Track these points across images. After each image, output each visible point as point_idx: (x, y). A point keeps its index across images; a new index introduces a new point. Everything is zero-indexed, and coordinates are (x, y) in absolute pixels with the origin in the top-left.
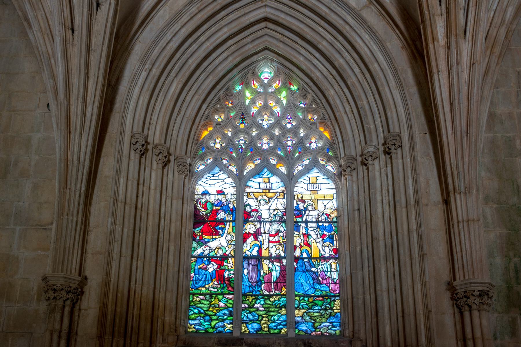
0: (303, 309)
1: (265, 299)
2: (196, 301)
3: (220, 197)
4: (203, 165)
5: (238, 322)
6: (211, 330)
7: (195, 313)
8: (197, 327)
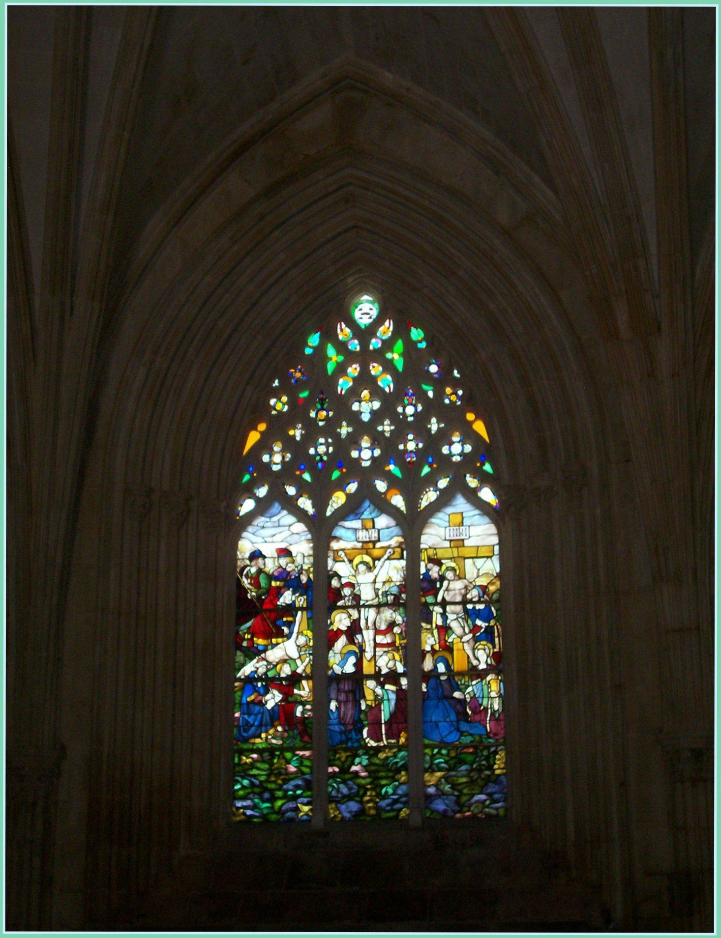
0: (440, 770)
2: (246, 763)
3: (283, 561)
4: (250, 498)
6: (273, 817)
8: (249, 812)
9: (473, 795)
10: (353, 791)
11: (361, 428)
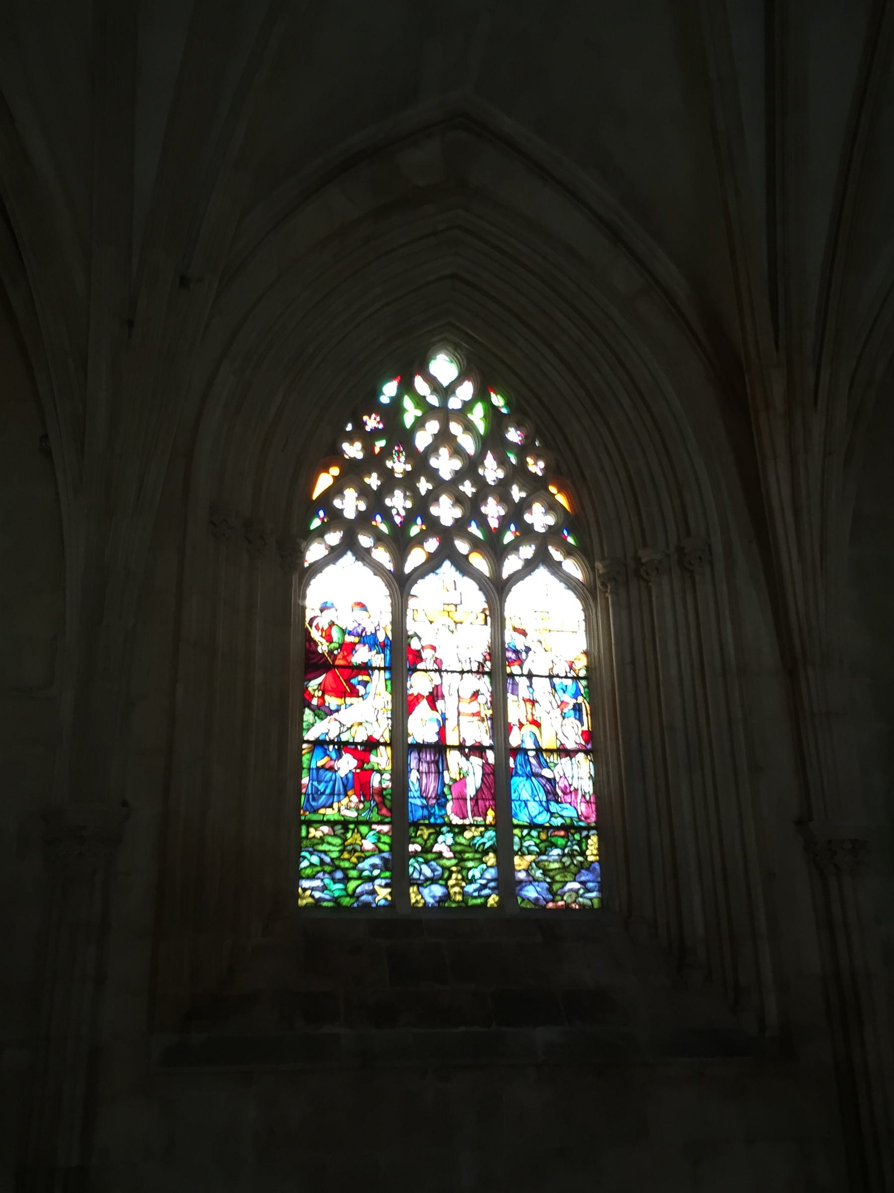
0: (530, 853)
1: (455, 834)
2: (314, 837)
5: (401, 882)
6: (346, 901)
7: (312, 865)
8: (317, 894)
9: (566, 882)
10: (436, 873)
11: (440, 486)
